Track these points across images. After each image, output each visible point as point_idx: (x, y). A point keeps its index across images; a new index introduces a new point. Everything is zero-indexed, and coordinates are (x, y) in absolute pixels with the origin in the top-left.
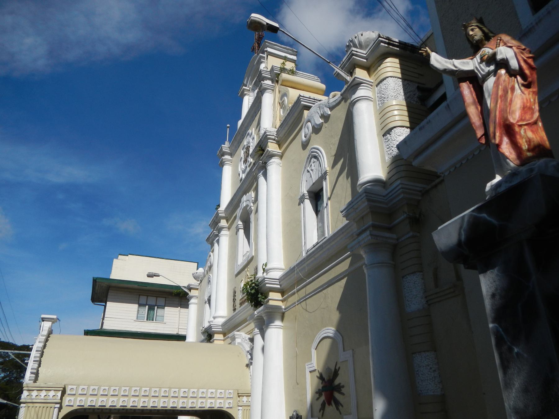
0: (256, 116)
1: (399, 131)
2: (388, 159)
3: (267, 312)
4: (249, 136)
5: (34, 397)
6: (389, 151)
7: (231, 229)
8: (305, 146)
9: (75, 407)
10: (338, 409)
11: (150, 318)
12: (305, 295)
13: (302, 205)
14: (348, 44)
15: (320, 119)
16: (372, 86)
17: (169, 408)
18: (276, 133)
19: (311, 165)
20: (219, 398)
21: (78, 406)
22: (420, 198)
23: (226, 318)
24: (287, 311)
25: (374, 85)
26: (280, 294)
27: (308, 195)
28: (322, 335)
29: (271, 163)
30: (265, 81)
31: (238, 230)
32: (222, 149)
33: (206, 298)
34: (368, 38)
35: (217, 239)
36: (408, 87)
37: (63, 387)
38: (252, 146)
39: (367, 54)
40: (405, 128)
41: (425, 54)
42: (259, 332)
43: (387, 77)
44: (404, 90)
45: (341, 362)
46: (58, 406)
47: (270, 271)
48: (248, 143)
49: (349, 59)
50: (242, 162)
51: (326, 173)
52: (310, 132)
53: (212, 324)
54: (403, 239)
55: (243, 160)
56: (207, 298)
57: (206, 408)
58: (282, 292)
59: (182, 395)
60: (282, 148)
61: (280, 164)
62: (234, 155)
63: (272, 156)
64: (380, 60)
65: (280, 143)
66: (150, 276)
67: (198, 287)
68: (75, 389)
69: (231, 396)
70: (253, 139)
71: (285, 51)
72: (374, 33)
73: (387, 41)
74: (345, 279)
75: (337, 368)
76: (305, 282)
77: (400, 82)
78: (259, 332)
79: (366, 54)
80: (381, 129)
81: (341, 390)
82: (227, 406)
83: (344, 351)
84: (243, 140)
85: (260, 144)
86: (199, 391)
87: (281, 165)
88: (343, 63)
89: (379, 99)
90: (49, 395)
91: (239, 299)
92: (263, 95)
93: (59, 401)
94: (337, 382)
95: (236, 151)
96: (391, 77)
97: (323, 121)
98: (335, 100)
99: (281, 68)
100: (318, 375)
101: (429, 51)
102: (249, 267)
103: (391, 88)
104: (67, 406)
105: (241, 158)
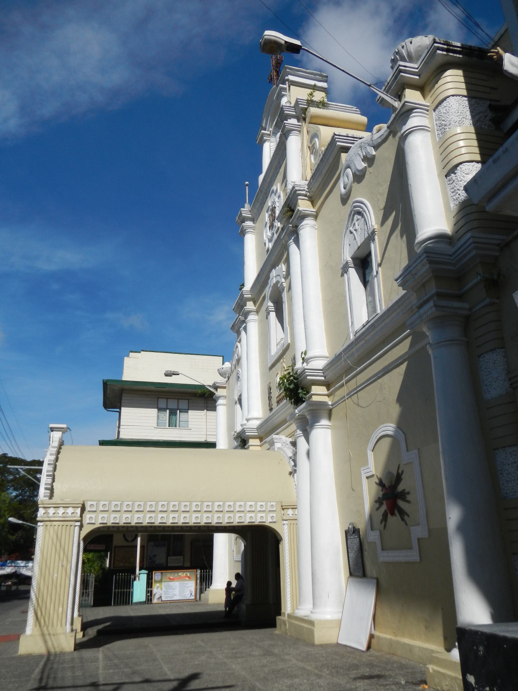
0: (280, 168)
1: (466, 168)
2: (453, 206)
3: (310, 410)
4: (273, 194)
5: (51, 514)
6: (455, 195)
7: (260, 313)
8: (345, 199)
9: (97, 525)
10: (403, 519)
11: (172, 424)
12: (355, 386)
13: (345, 275)
14: (393, 58)
15: (363, 163)
16: (428, 111)
17: (202, 524)
18: (307, 187)
19: (354, 224)
20: (259, 511)
21: (101, 523)
22: (498, 254)
23: (262, 420)
24: (334, 407)
25: (431, 109)
26: (325, 387)
27: (352, 262)
28: (380, 433)
29: (303, 225)
30: (288, 120)
31: (268, 313)
32: (241, 214)
33: (236, 398)
34: (419, 46)
35: (244, 326)
36: (476, 107)
37: (82, 503)
38: (278, 206)
39: (419, 68)
40: (474, 163)
41: (495, 57)
42: (302, 434)
43: (448, 97)
44: (472, 112)
45: (404, 465)
46: (79, 524)
47: (309, 360)
48: (273, 203)
49: (396, 78)
50: (268, 228)
51: (373, 232)
52: (351, 182)
53: (245, 427)
54: (478, 308)
55: (268, 225)
56: (237, 398)
57: (246, 523)
58: (328, 385)
59: (216, 509)
60: (315, 206)
61: (315, 227)
62: (257, 220)
63: (303, 217)
64: (437, 75)
65: (313, 199)
66: (168, 374)
67: (225, 385)
68: (95, 505)
69: (274, 509)
70: (279, 197)
71: (311, 77)
72: (428, 38)
73: (445, 47)
74: (405, 364)
75: (400, 472)
76: (355, 371)
77: (465, 102)
78: (302, 434)
79: (417, 69)
80: (443, 167)
81: (406, 497)
82: (270, 520)
83: (408, 451)
84: (266, 200)
85: (288, 203)
86: (235, 504)
87: (316, 227)
88: (388, 84)
89: (438, 127)
90: (67, 513)
91: (276, 396)
92: (287, 139)
93: (79, 519)
94: (400, 488)
95: (259, 215)
96: (453, 96)
97: (366, 165)
98: (381, 136)
99: (308, 100)
100: (377, 481)
101: (501, 51)
102: (284, 357)
103: (453, 111)
104: (88, 523)
105: (266, 223)
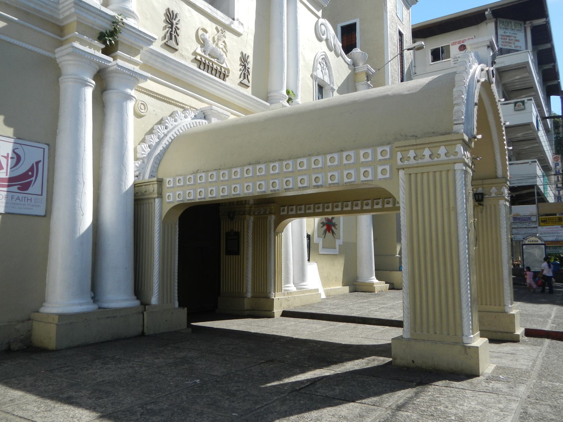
10: (333, 235)
